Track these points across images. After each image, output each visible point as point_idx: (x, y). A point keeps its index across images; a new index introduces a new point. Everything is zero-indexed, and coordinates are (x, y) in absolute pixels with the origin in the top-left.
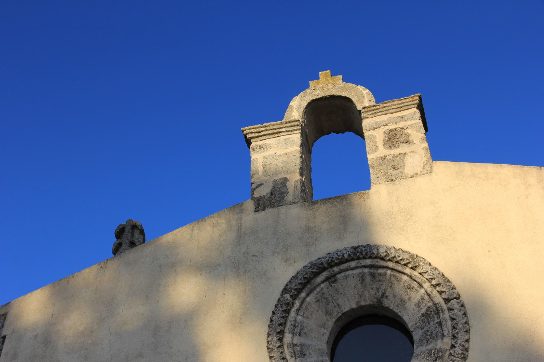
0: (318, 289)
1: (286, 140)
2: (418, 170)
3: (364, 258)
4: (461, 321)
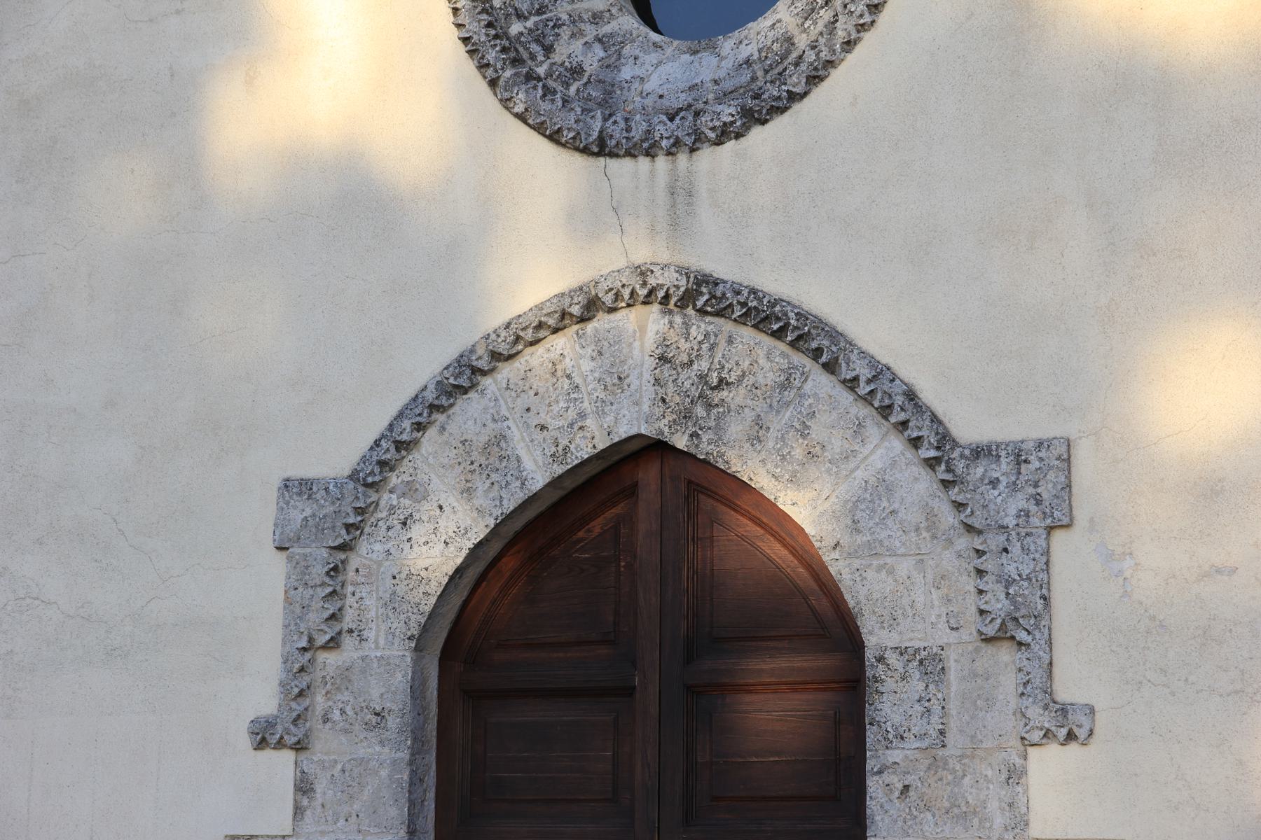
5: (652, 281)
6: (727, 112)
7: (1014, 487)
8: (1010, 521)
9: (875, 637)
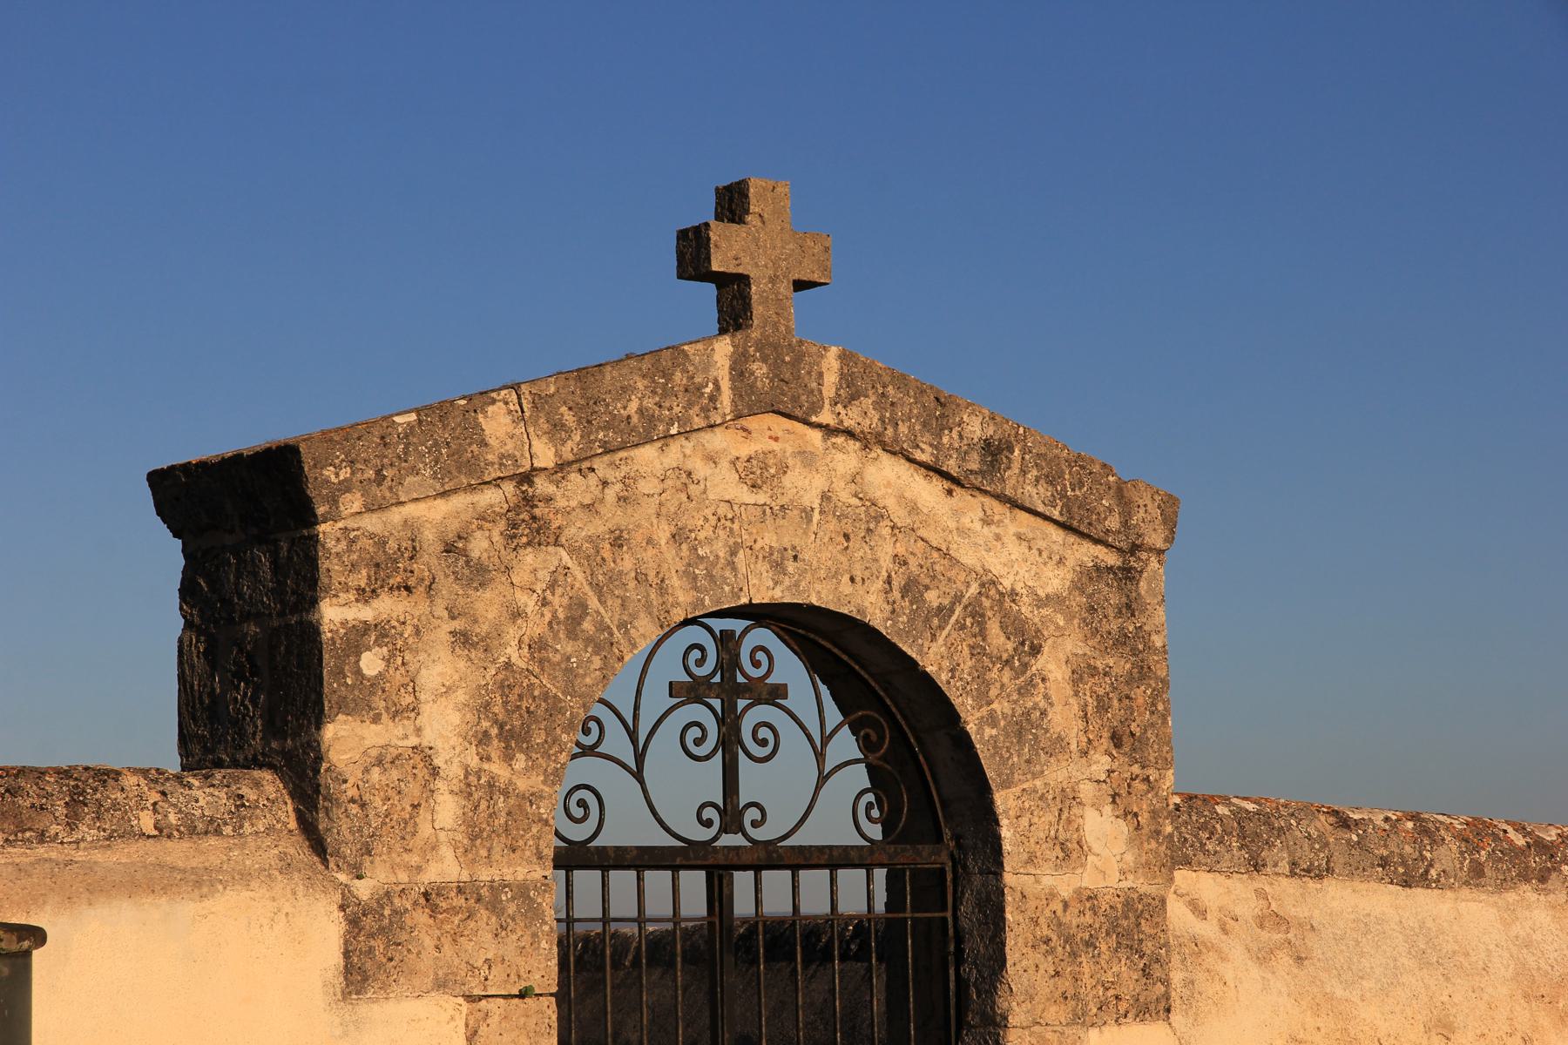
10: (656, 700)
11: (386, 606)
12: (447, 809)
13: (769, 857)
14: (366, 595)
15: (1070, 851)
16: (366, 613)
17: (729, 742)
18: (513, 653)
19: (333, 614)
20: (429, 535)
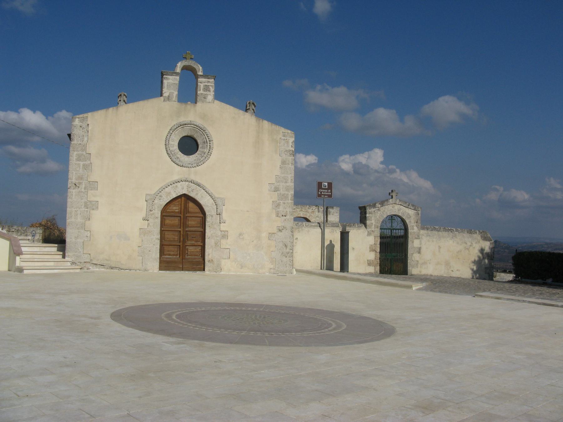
0: (179, 130)
1: (174, 78)
2: (210, 101)
3: (192, 125)
4: (212, 147)
5: (187, 180)
6: (195, 165)
7: (220, 202)
8: (220, 204)
9: (207, 214)
10: (387, 220)
11: (370, 215)
12: (373, 226)
13: (394, 229)
14: (369, 214)
15: (413, 229)
16: (369, 215)
17: (392, 222)
18: (377, 217)
19: (367, 215)
20: (373, 211)
